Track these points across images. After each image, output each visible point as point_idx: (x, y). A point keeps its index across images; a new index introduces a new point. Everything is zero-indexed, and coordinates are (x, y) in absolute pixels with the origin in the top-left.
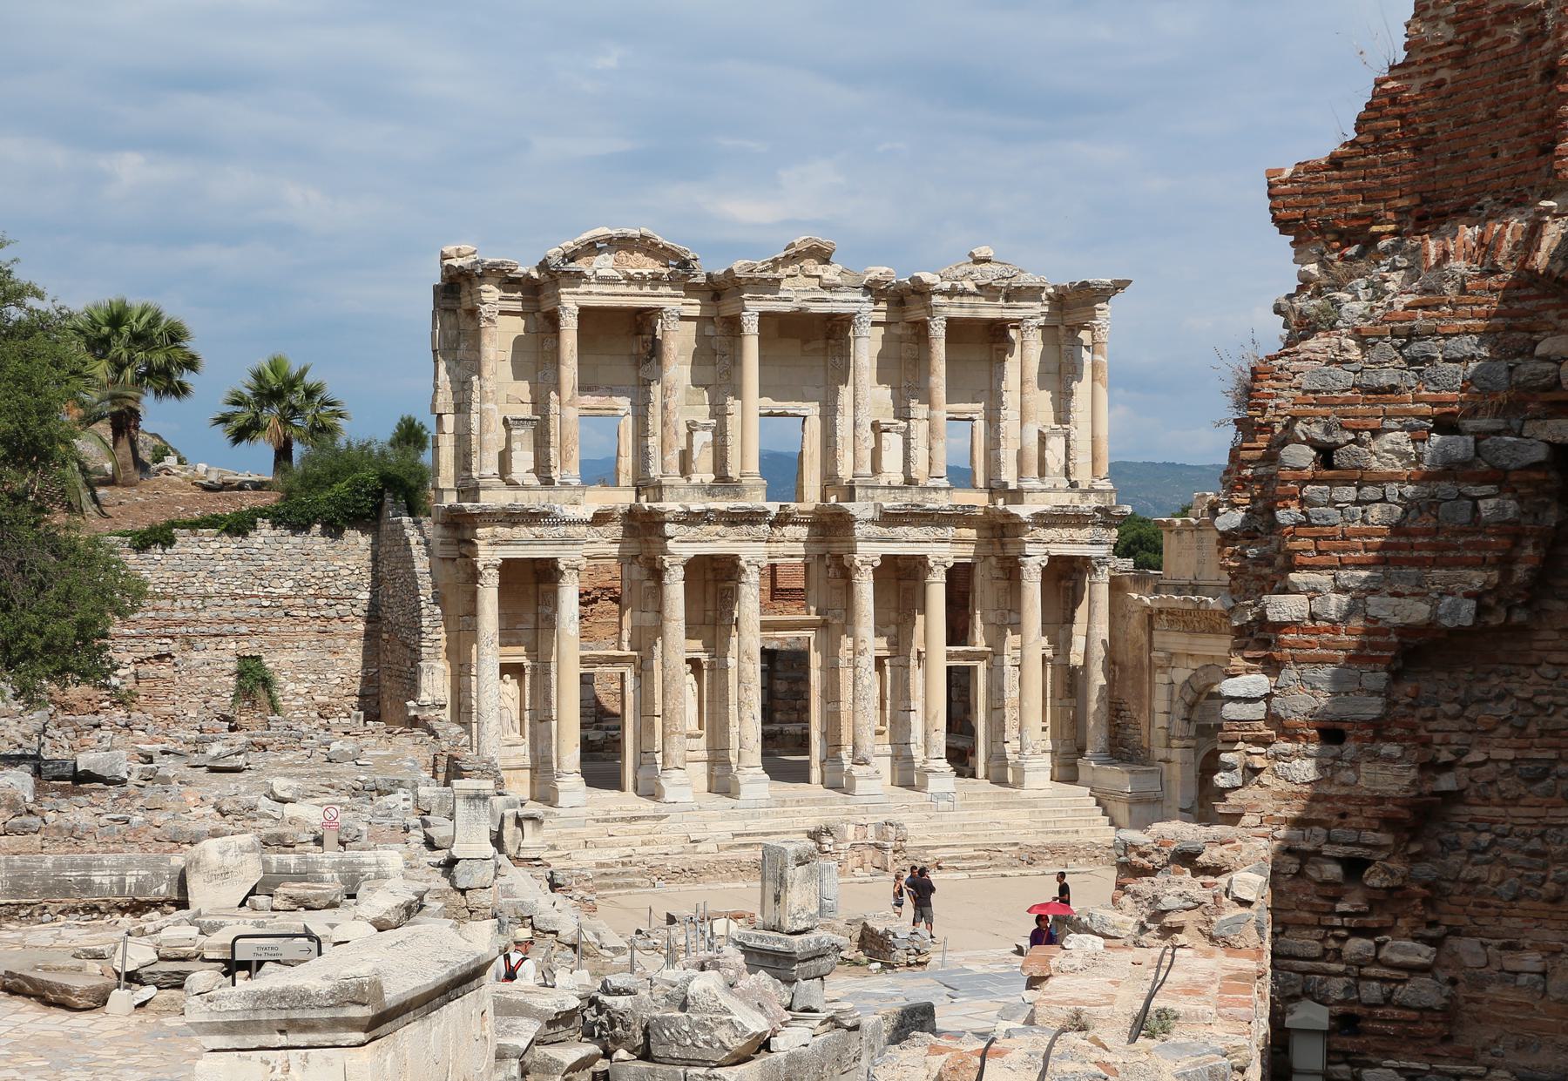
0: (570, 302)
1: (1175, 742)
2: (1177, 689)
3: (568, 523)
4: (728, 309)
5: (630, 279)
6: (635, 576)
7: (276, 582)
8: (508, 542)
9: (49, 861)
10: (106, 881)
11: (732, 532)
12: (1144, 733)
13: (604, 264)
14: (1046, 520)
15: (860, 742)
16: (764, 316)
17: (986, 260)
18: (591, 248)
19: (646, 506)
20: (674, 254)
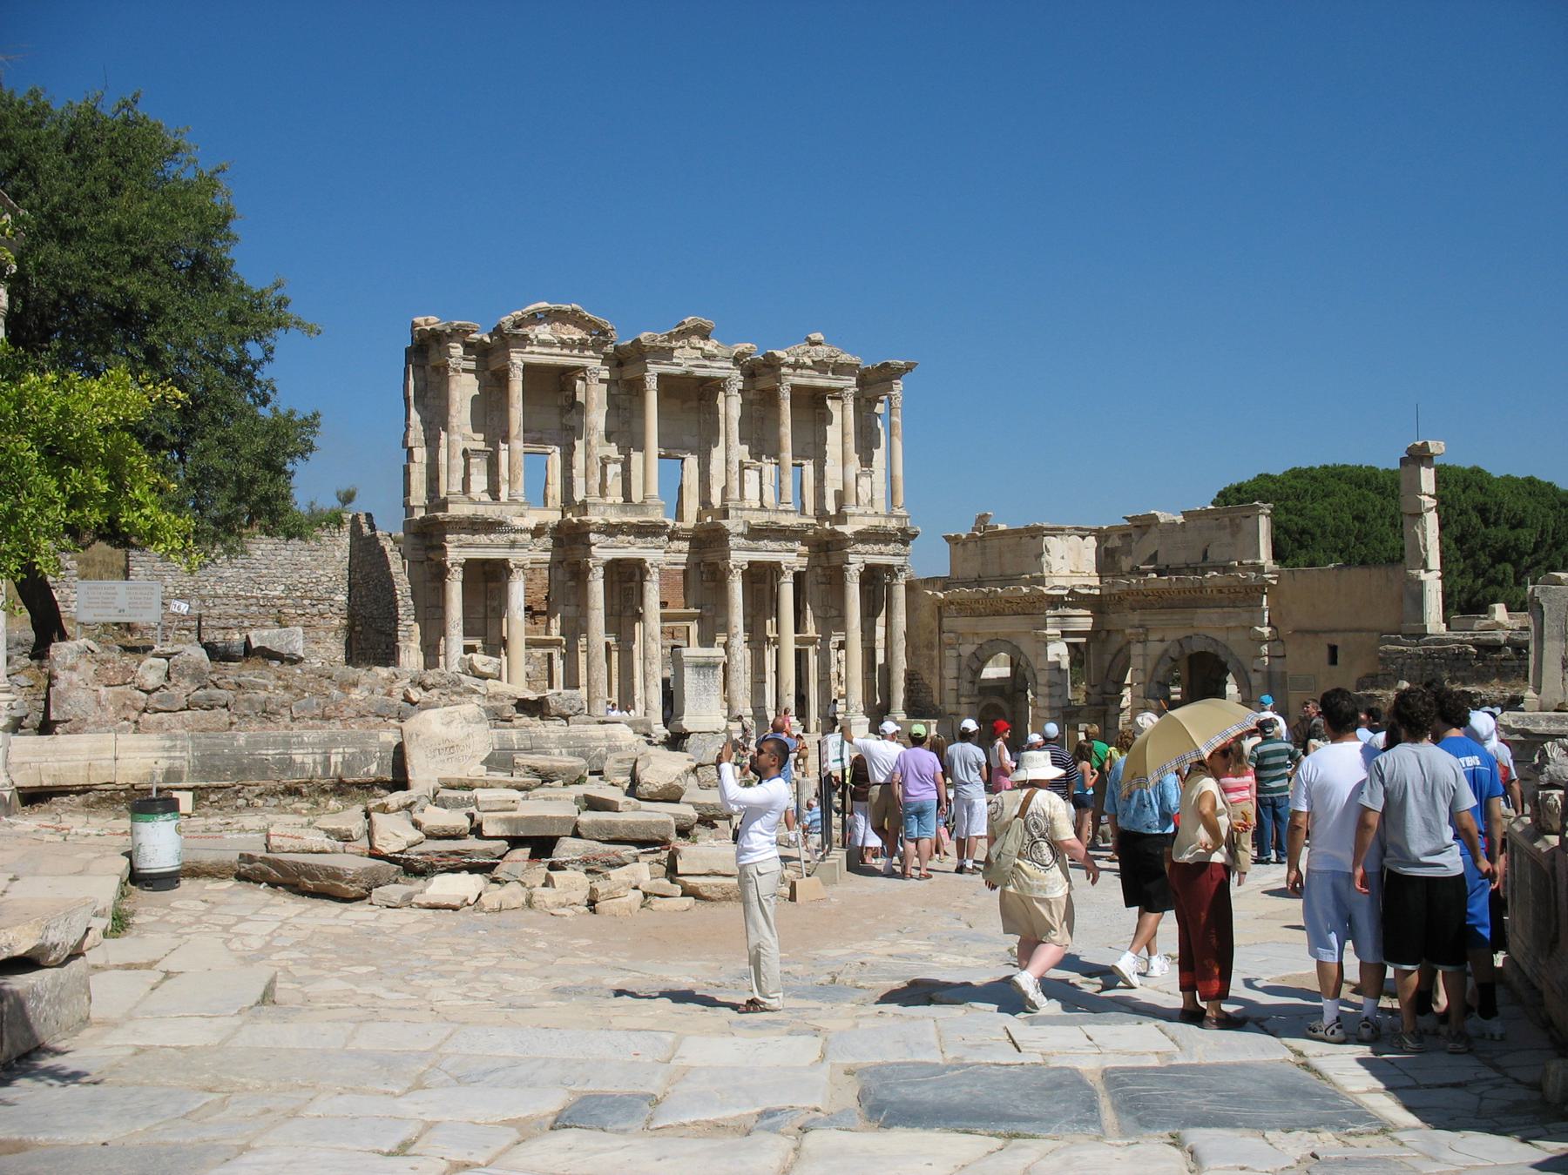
0: (518, 359)
1: (963, 700)
2: (964, 661)
3: (517, 531)
4: (630, 373)
5: (563, 344)
6: (560, 577)
7: (271, 587)
8: (470, 546)
9: (242, 739)
10: (309, 760)
11: (640, 542)
12: (936, 694)
13: (543, 332)
14: (865, 537)
15: (734, 704)
16: (659, 375)
17: (819, 343)
18: (534, 319)
19: (575, 520)
20: (597, 326)
